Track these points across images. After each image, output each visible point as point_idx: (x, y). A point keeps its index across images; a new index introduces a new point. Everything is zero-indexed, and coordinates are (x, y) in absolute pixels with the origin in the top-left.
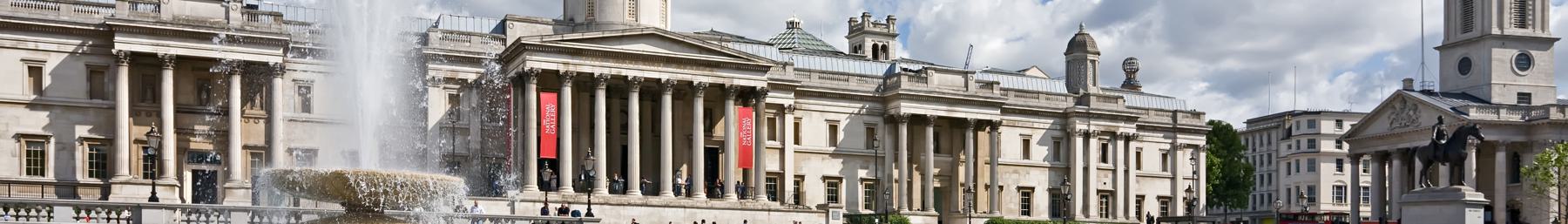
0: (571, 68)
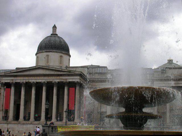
0: (14, 81)
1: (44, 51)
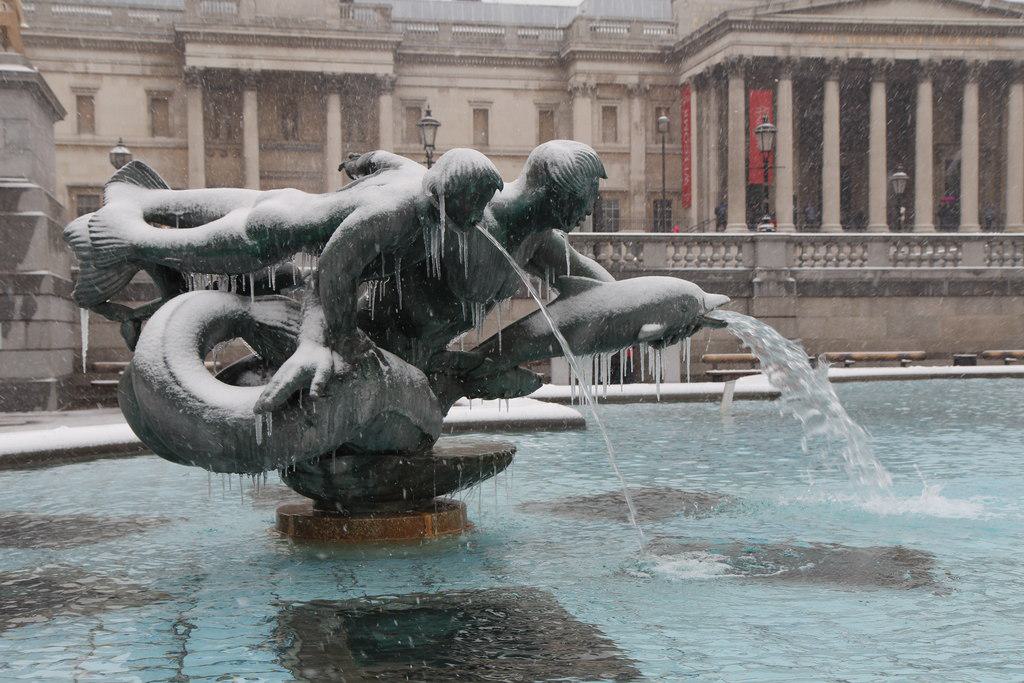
0: (793, 52)
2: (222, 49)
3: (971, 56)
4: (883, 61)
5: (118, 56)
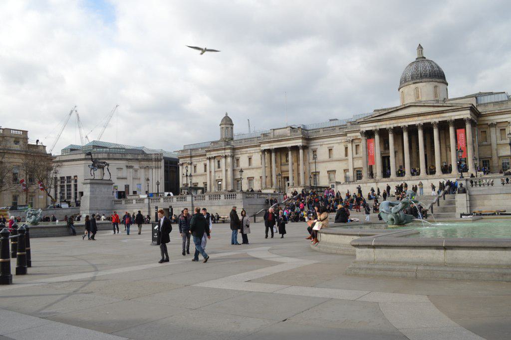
0: (378, 128)
1: (410, 83)
2: (267, 145)
3: (432, 121)
4: (405, 126)
5: (255, 148)
